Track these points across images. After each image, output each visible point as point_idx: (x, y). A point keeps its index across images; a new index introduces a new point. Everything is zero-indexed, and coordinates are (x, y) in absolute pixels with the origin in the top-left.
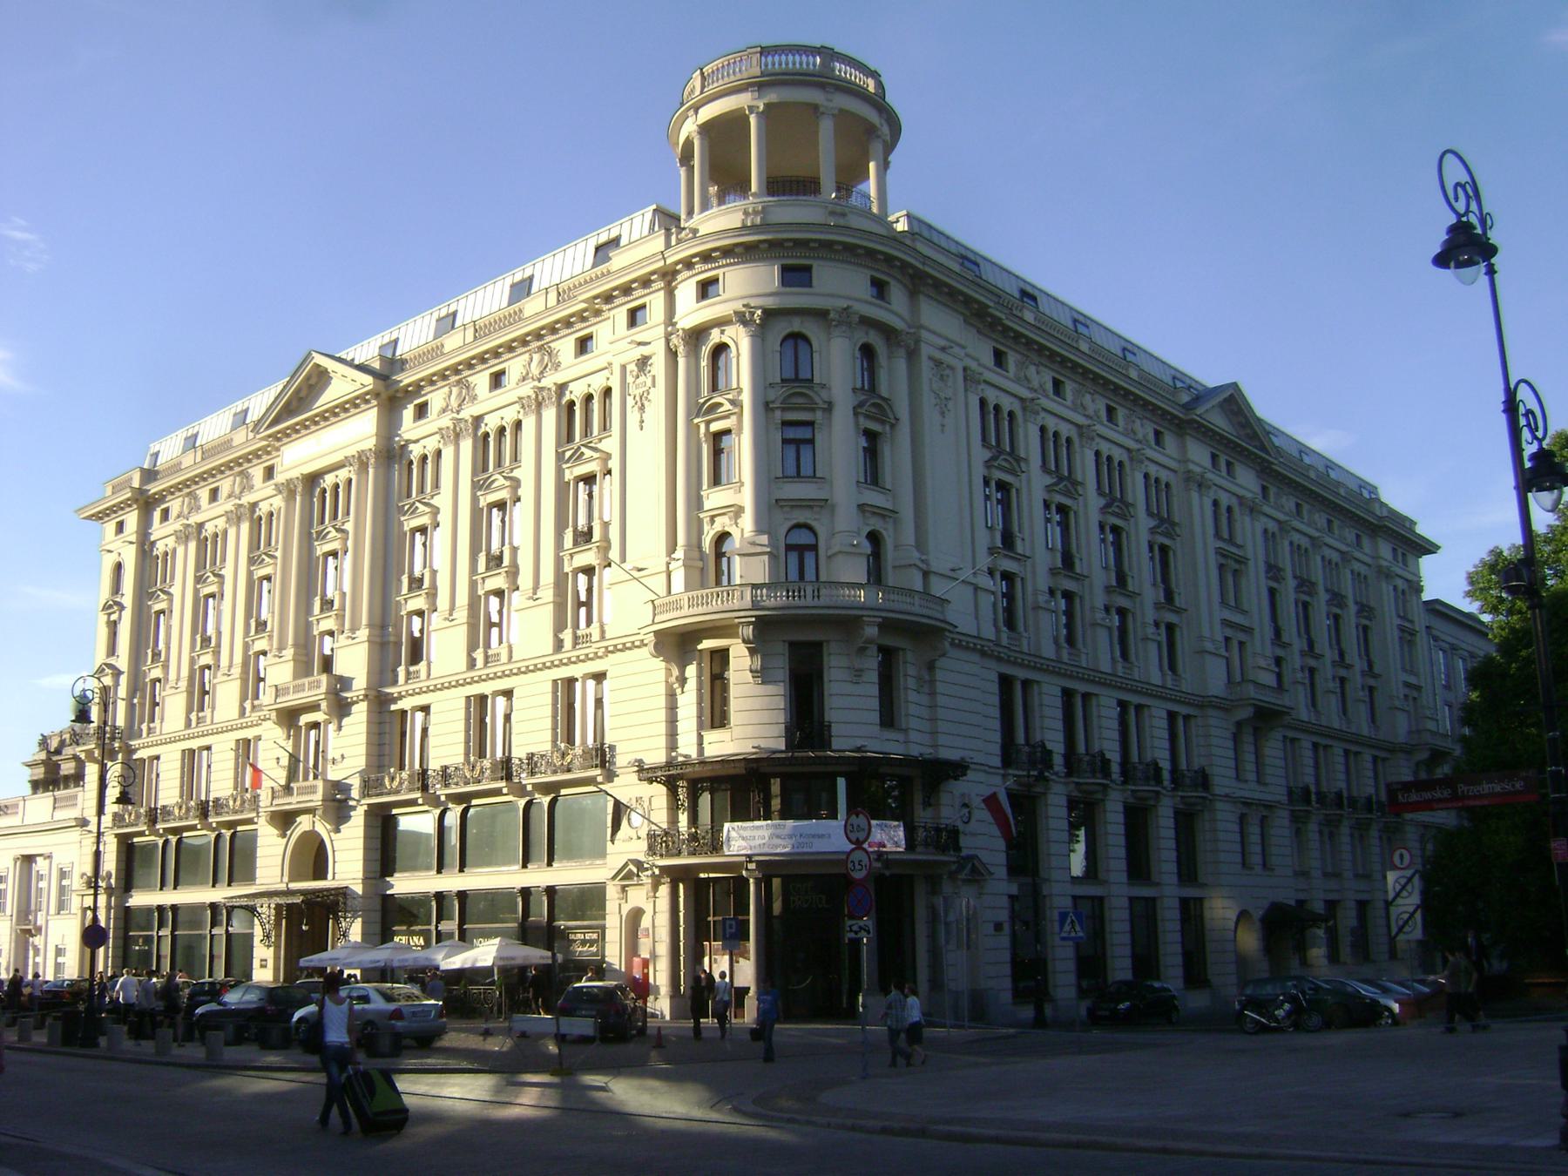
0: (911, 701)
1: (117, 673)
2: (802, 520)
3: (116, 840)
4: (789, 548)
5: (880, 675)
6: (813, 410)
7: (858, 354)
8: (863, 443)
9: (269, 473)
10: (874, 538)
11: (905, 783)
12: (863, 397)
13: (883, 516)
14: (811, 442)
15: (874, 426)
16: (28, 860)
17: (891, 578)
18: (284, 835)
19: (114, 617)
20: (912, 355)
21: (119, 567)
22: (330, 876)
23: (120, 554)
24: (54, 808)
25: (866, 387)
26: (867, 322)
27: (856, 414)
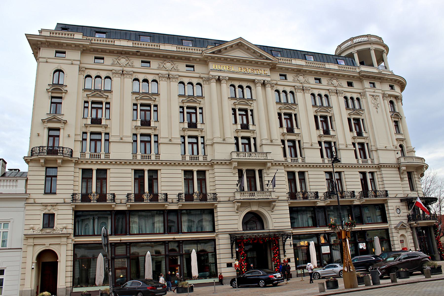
5: (409, 178)
7: (389, 103)
8: (394, 124)
10: (401, 146)
12: (392, 113)
13: (402, 141)
15: (397, 120)
17: (407, 155)
25: (393, 111)
26: (390, 96)
27: (391, 118)
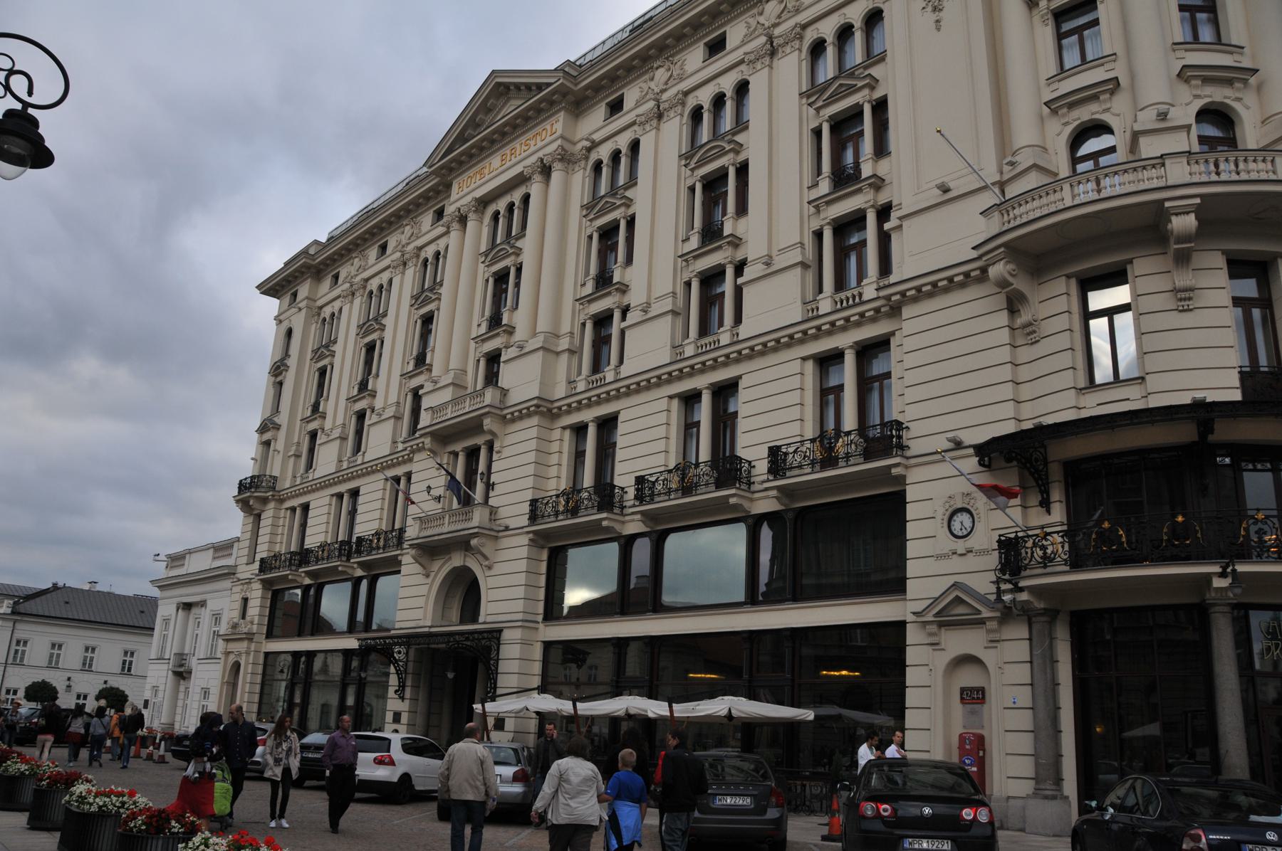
1: (277, 427)
3: (260, 586)
9: (440, 214)
16: (188, 607)
18: (428, 576)
19: (279, 379)
21: (289, 333)
22: (481, 619)
23: (290, 321)
24: (214, 558)
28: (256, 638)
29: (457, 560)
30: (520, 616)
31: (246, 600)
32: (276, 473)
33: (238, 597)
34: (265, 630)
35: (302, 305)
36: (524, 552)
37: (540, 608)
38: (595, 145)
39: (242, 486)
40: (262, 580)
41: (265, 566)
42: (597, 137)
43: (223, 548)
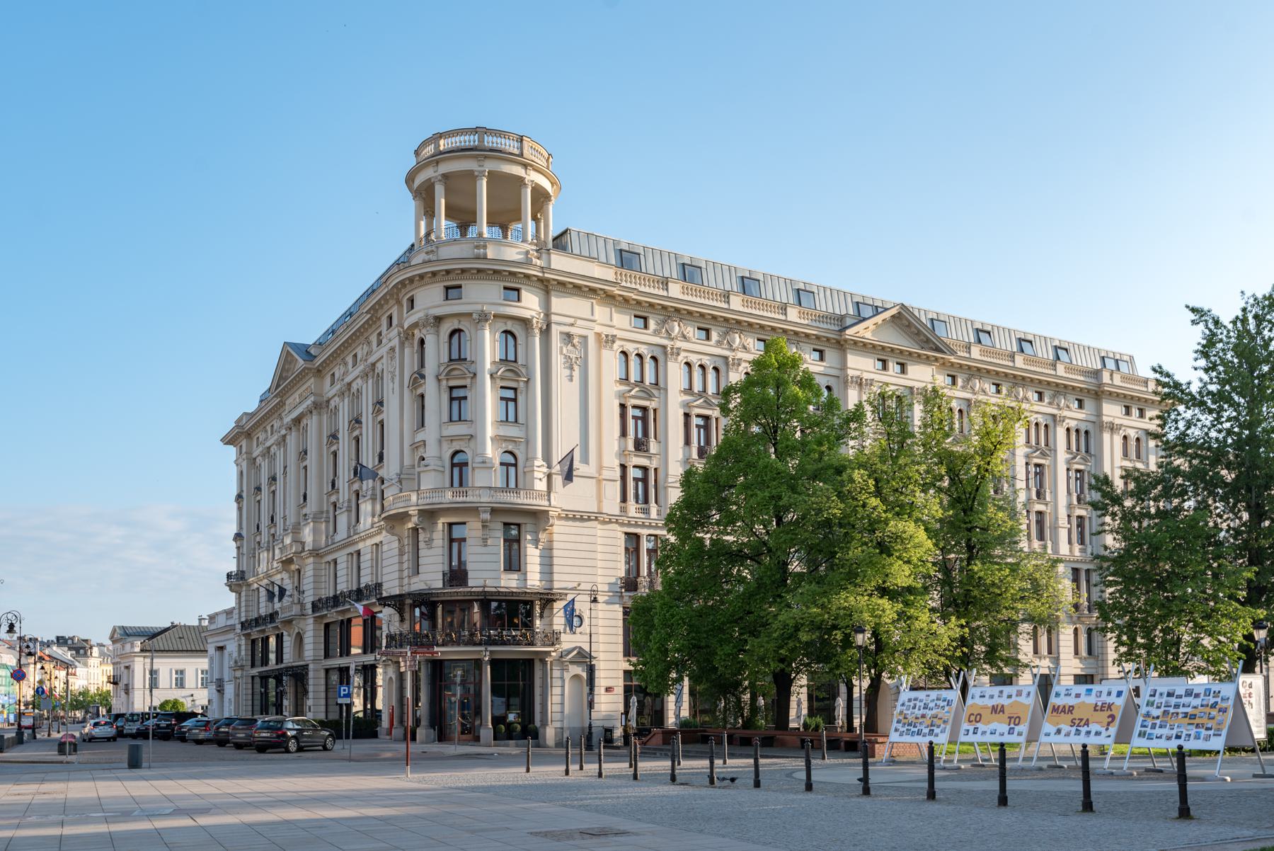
0: (532, 556)
2: (458, 448)
4: (453, 465)
6: (465, 378)
11: (532, 603)
14: (465, 398)
16: (221, 649)
20: (546, 333)
21: (242, 472)
28: (246, 668)
29: (296, 631)
30: (312, 658)
31: (240, 645)
32: (245, 569)
33: (236, 644)
34: (250, 663)
35: (245, 456)
36: (311, 627)
37: (322, 653)
38: (328, 401)
39: (229, 576)
40: (244, 635)
41: (244, 625)
42: (330, 394)
43: (229, 613)
